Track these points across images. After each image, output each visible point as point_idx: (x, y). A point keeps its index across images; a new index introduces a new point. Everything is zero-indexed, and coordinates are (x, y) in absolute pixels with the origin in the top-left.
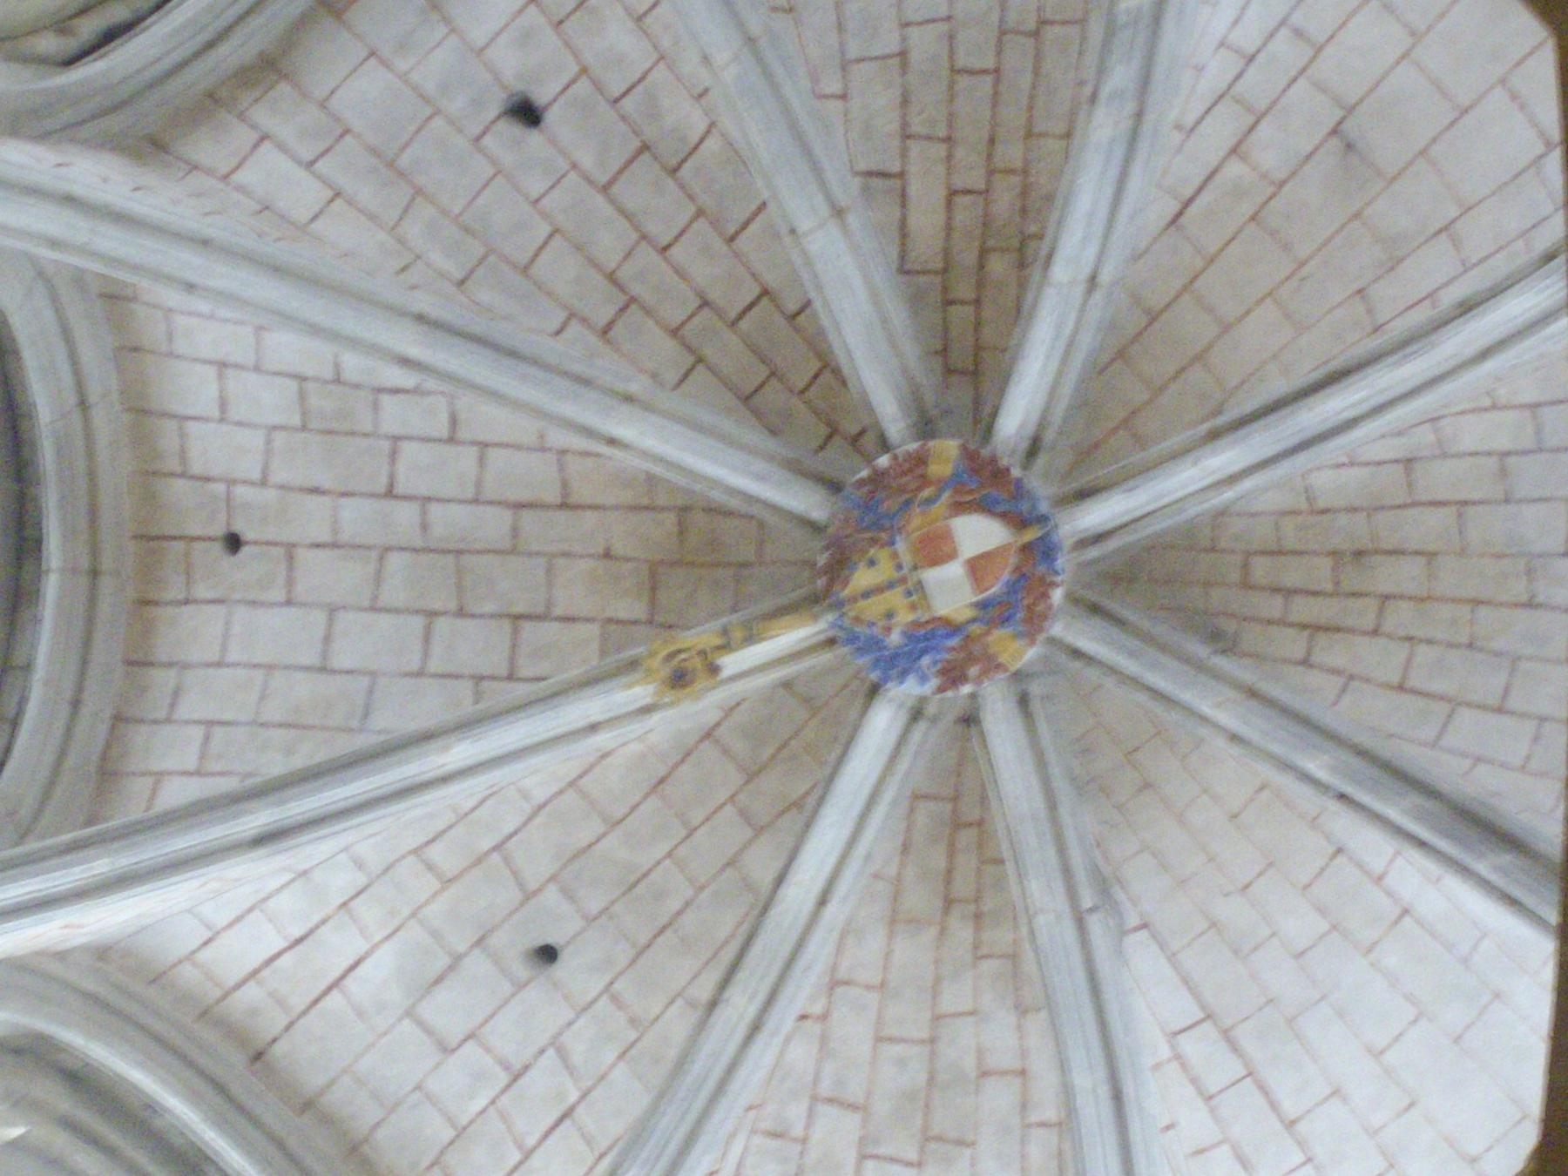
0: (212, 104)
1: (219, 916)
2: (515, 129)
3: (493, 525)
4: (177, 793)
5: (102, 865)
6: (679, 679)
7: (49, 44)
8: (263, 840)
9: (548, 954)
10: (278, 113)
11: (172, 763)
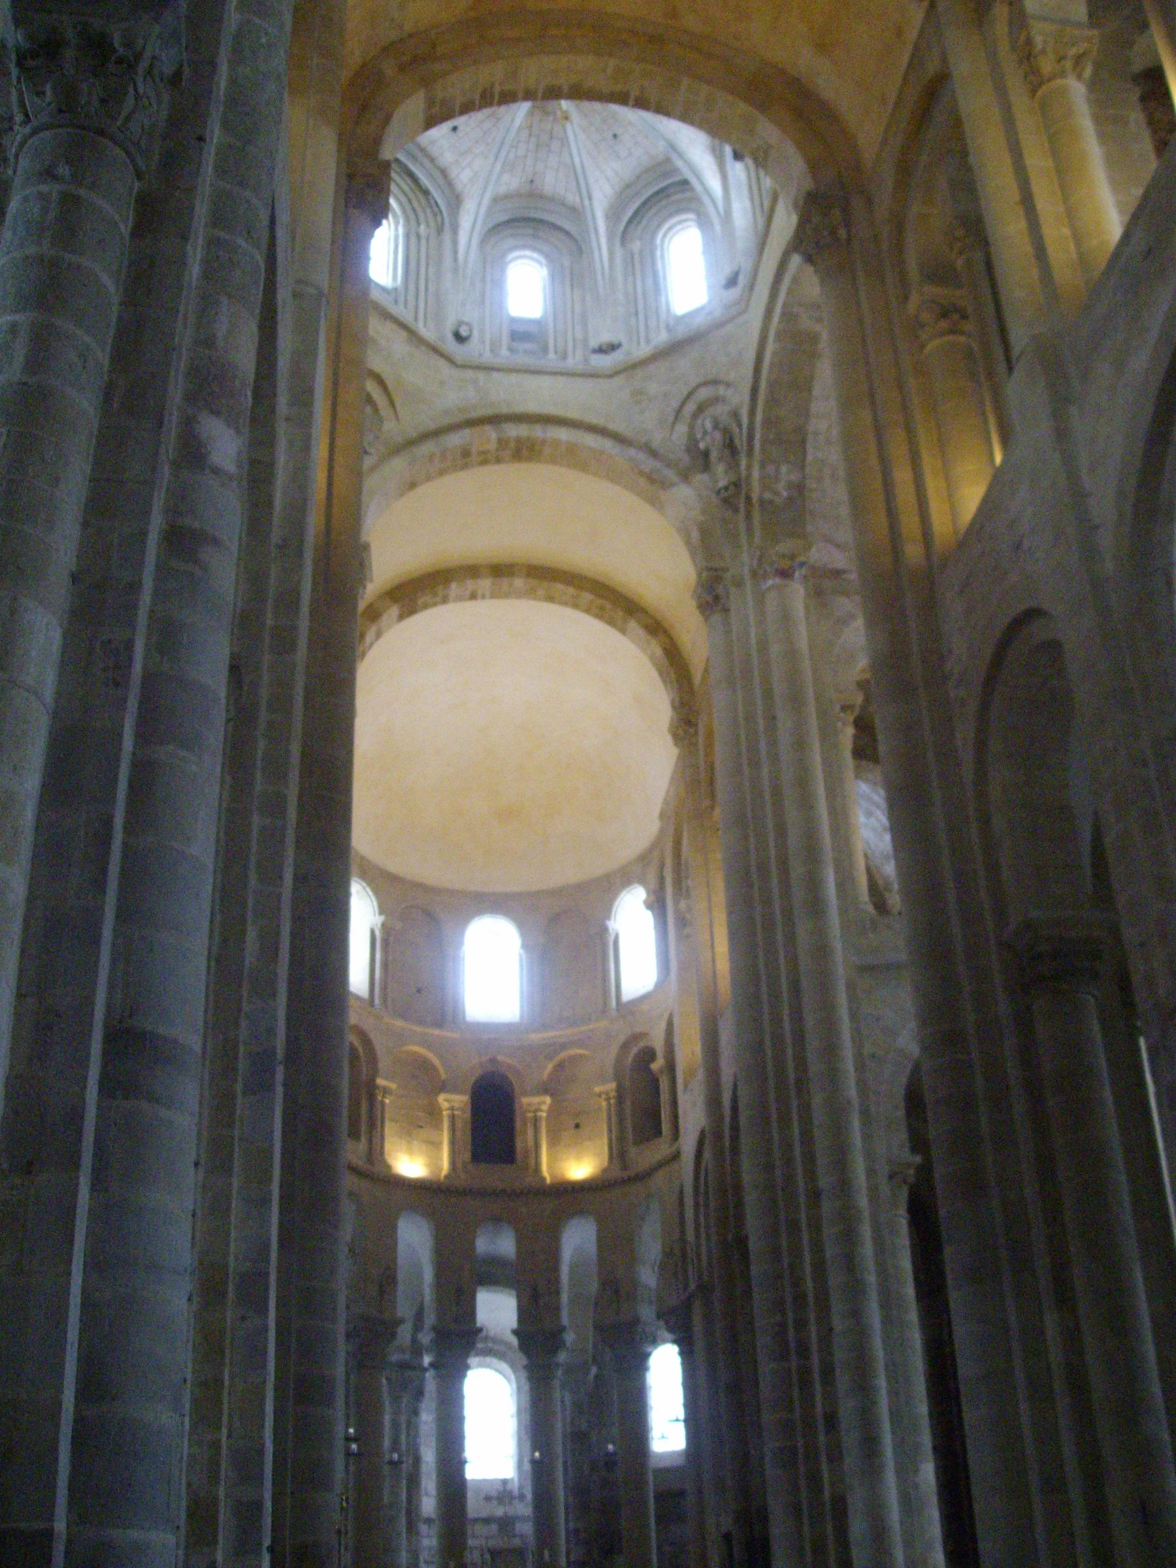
0: (450, 184)
1: (601, 194)
2: (458, 132)
3: (533, 139)
4: (578, 199)
5: (593, 236)
6: (567, 118)
7: (439, 219)
8: (590, 199)
9: (615, 136)
10: (453, 173)
11: (572, 198)
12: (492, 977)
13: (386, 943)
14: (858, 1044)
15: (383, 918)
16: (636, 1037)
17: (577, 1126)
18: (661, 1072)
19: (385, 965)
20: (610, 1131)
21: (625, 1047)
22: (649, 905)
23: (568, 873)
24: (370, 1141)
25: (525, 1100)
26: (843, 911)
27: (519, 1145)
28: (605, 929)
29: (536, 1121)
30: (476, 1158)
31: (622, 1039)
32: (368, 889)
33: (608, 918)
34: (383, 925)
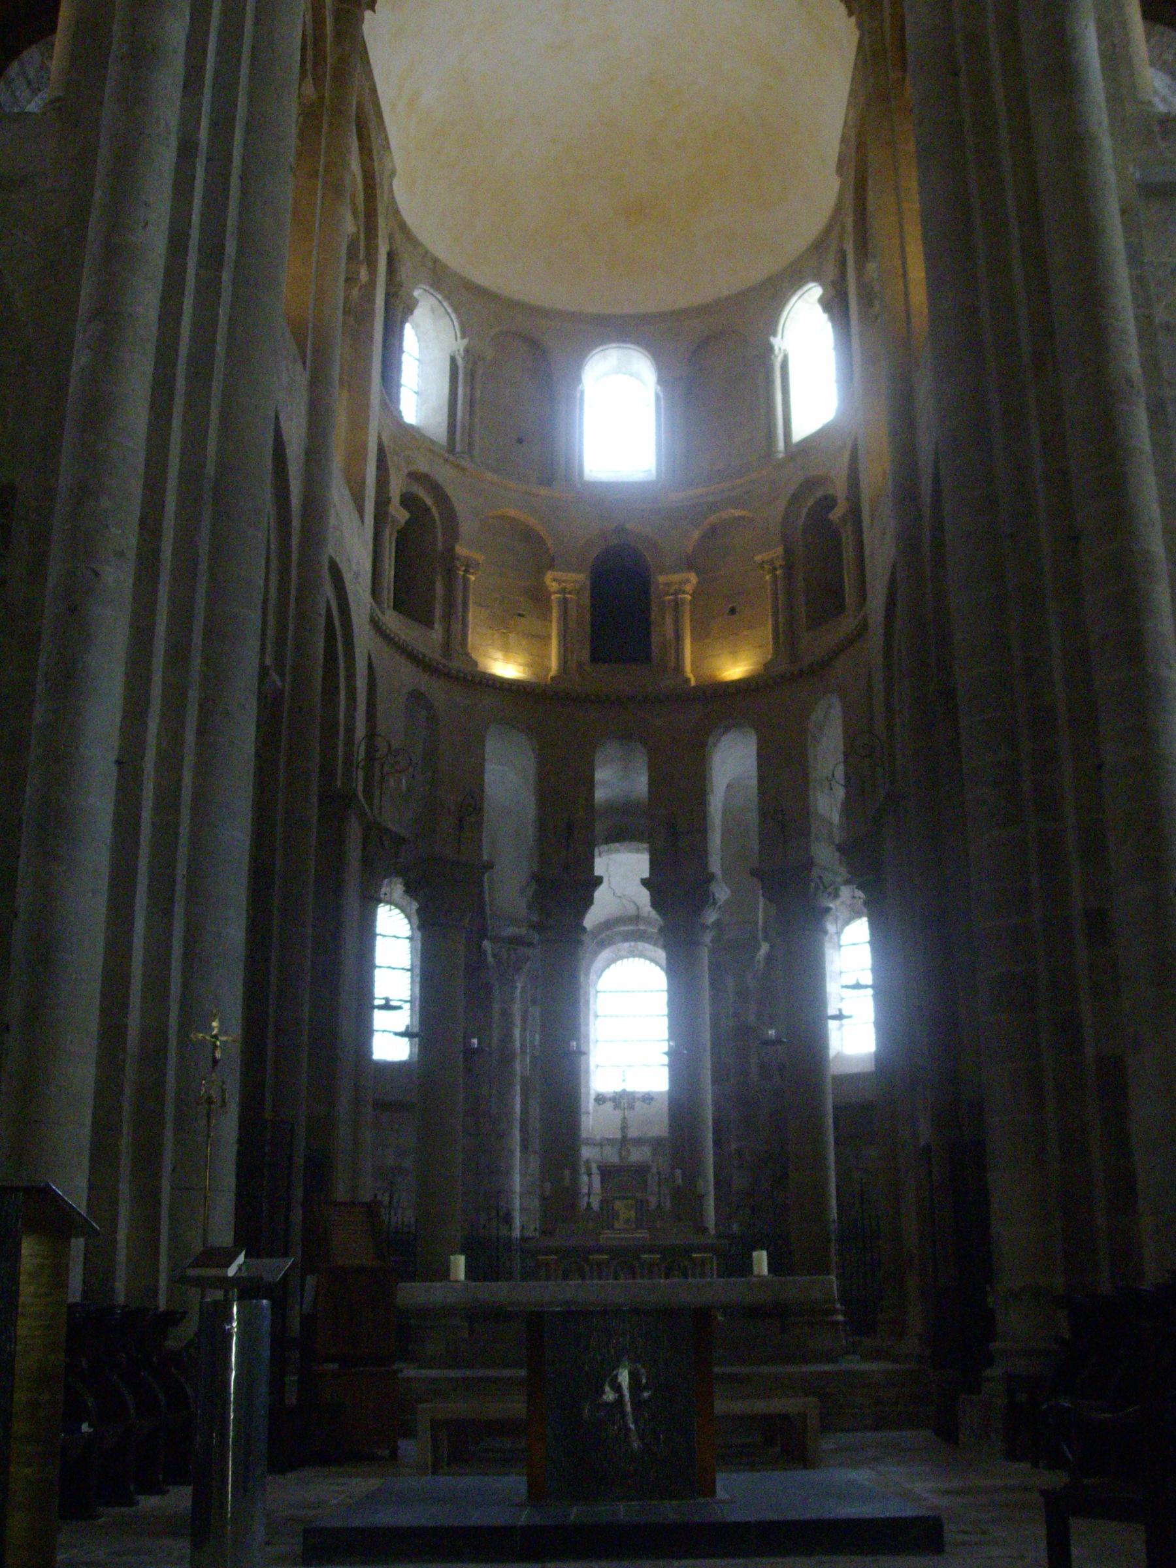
12: (619, 425)
13: (471, 375)
14: (1144, 303)
15: (466, 341)
16: (810, 484)
17: (733, 611)
18: (843, 519)
19: (471, 403)
20: (775, 615)
21: (795, 498)
22: (827, 304)
23: (719, 281)
24: (448, 630)
25: (661, 579)
26: (1114, 99)
27: (655, 639)
28: (770, 348)
29: (677, 605)
30: (595, 658)
31: (793, 486)
32: (446, 304)
33: (774, 334)
34: (467, 351)
